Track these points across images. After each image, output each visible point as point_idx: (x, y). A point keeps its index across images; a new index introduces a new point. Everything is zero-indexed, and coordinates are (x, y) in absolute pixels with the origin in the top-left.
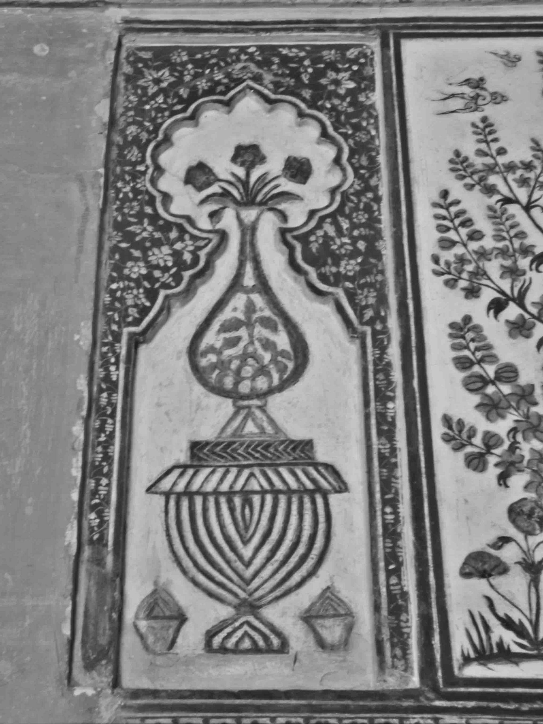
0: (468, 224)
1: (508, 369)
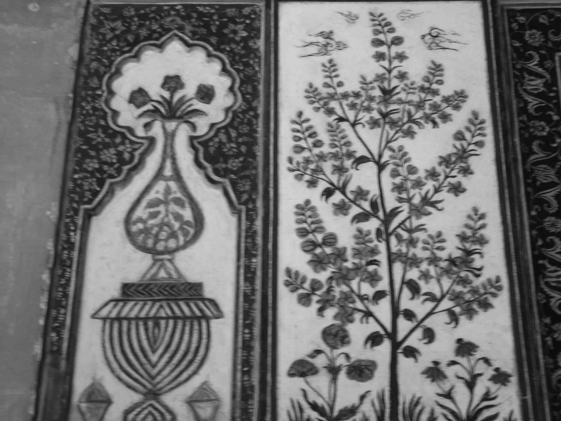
0: (314, 135)
1: (330, 237)
